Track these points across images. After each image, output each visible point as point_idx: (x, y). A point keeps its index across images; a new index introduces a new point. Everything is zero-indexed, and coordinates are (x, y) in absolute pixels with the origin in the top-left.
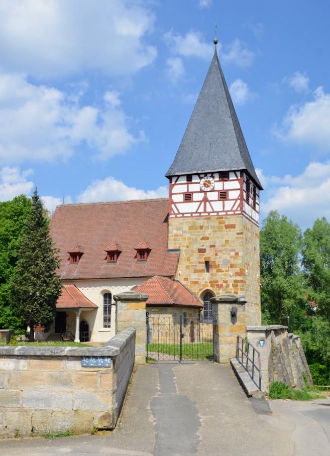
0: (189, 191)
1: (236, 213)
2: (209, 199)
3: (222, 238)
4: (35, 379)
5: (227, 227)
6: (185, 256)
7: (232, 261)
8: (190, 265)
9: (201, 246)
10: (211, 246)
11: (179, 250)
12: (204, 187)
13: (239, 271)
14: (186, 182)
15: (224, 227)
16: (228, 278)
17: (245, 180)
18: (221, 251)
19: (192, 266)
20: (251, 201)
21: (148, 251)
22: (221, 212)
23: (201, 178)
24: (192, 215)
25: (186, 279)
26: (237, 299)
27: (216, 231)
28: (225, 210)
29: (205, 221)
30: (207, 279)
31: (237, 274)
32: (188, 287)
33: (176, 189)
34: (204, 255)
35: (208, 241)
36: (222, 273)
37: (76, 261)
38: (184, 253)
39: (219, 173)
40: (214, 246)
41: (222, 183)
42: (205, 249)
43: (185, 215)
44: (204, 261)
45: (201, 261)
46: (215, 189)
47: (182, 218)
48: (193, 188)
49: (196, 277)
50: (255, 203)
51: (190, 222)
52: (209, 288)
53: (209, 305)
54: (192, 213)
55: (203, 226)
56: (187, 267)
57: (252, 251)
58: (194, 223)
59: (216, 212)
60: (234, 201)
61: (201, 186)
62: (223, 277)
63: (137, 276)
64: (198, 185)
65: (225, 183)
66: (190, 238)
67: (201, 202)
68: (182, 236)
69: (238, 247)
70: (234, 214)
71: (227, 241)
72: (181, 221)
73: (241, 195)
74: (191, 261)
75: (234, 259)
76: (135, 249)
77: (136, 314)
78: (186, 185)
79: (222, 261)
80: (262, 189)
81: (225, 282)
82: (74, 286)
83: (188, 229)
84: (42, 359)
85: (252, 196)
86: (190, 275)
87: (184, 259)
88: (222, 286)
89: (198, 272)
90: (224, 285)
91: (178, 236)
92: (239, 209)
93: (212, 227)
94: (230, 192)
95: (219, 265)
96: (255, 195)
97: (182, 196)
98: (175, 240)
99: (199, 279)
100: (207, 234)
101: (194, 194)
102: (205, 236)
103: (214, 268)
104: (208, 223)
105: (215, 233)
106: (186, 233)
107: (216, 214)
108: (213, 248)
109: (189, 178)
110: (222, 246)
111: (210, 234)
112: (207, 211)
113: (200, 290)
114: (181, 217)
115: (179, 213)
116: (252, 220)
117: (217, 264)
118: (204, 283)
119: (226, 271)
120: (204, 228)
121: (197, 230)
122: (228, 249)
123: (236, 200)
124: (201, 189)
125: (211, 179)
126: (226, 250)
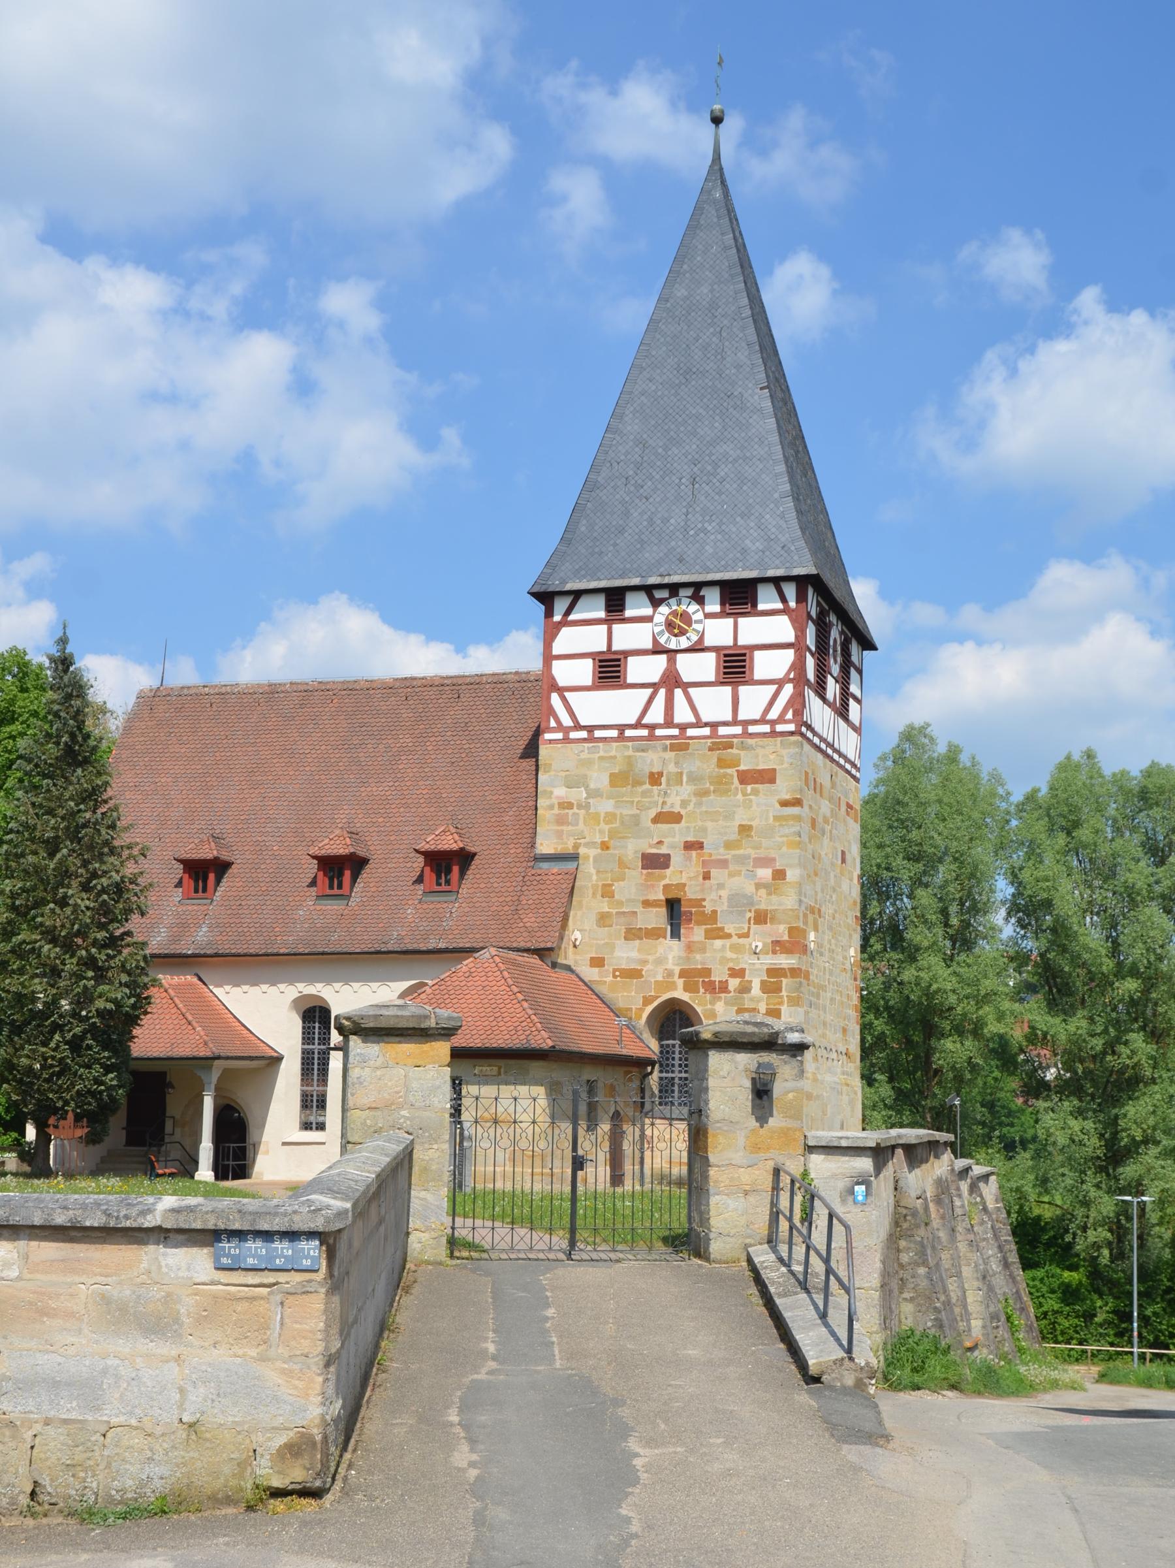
0: (615, 648)
1: (780, 728)
2: (686, 678)
3: (729, 816)
4: (44, 1312)
5: (745, 778)
6: (594, 877)
7: (764, 901)
8: (614, 911)
9: (650, 846)
10: (689, 846)
11: (574, 857)
12: (667, 635)
13: (786, 938)
14: (602, 614)
15: (736, 780)
16: (746, 961)
17: (814, 614)
18: (723, 863)
19: (617, 913)
20: (832, 688)
21: (464, 858)
22: (725, 724)
23: (656, 603)
24: (622, 732)
25: (598, 962)
26: (777, 1034)
27: (706, 793)
28: (741, 717)
29: (670, 755)
30: (670, 961)
31: (778, 946)
32: (602, 990)
33: (566, 641)
34: (665, 877)
36: (727, 942)
37: (205, 890)
38: (593, 871)
39: (723, 585)
40: (699, 846)
41: (730, 621)
42: (667, 857)
43: (598, 734)
44: (662, 898)
45: (652, 897)
46: (708, 642)
48: (628, 636)
49: (634, 954)
50: (845, 694)
51: (615, 757)
53: (677, 1056)
54: (621, 728)
55: (661, 774)
56: (603, 919)
57: (832, 864)
58: (629, 761)
59: (706, 725)
60: (774, 687)
61: (657, 629)
62: (729, 955)
63: (423, 947)
64: (647, 626)
65: (742, 621)
66: (614, 815)
67: (655, 687)
68: (587, 806)
69: (784, 849)
70: (773, 734)
71: (745, 829)
72: (584, 756)
73: (798, 666)
74: (617, 897)
75: (769, 894)
76: (417, 851)
77: (414, 1085)
78: (604, 627)
79: (725, 900)
80: (874, 648)
81: (738, 973)
82: (195, 980)
84: (72, 1240)
85: (835, 669)
86: (612, 947)
87: (590, 892)
89: (642, 939)
90: (734, 983)
91: (570, 806)
92: (789, 716)
93: (693, 779)
94: (758, 655)
95: (715, 912)
96: (846, 666)
97: (588, 665)
98: (561, 821)
99: (646, 962)
100: (674, 802)
101: (631, 660)
103: (699, 923)
104: (677, 763)
105: (704, 799)
106: (601, 796)
107: (706, 731)
108: (694, 853)
109: (615, 600)
110: (728, 845)
111: (684, 803)
113: (647, 1001)
114: (584, 740)
115: (578, 727)
116: (836, 757)
117: (708, 909)
118: (660, 978)
119: (740, 936)
120: (664, 780)
121: (640, 789)
122: (749, 857)
123: (780, 683)
124: (655, 641)
125: (693, 607)
126: (741, 860)
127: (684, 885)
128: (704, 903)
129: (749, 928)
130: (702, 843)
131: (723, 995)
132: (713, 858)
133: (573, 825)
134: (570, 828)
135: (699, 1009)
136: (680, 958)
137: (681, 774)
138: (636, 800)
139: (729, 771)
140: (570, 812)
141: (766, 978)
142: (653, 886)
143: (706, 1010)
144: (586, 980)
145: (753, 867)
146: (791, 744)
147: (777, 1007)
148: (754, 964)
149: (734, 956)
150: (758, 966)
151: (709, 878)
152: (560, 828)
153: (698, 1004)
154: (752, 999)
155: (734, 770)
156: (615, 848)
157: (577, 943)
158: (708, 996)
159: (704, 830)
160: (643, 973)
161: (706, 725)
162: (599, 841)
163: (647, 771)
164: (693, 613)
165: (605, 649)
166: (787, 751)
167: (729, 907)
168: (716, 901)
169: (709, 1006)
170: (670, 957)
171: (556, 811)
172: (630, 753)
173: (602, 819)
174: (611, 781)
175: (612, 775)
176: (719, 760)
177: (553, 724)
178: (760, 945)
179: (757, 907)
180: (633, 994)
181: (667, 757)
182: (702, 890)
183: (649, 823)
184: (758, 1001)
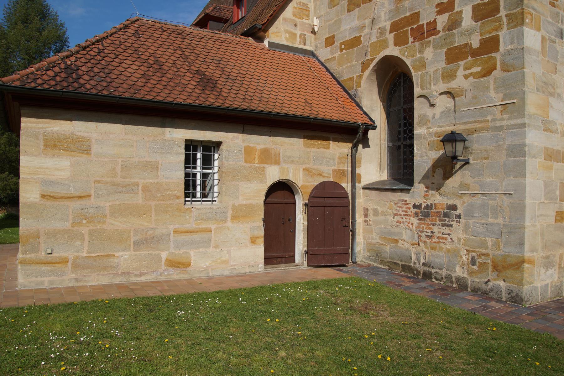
32: (333, 67)
49: (356, 23)
52: (392, 50)
86: (338, 22)
88: (432, 29)
90: (442, 20)
99: (362, 27)
113: (365, 66)
131: (431, 39)
135: (408, 62)
136: (390, 11)
144: (322, 60)
147: (495, 33)
153: (408, 57)
154: (462, 34)
157: (316, 29)
158: (417, 44)
160: (362, 39)
169: (418, 55)
170: (382, 14)
180: (354, 62)
184: (470, 34)
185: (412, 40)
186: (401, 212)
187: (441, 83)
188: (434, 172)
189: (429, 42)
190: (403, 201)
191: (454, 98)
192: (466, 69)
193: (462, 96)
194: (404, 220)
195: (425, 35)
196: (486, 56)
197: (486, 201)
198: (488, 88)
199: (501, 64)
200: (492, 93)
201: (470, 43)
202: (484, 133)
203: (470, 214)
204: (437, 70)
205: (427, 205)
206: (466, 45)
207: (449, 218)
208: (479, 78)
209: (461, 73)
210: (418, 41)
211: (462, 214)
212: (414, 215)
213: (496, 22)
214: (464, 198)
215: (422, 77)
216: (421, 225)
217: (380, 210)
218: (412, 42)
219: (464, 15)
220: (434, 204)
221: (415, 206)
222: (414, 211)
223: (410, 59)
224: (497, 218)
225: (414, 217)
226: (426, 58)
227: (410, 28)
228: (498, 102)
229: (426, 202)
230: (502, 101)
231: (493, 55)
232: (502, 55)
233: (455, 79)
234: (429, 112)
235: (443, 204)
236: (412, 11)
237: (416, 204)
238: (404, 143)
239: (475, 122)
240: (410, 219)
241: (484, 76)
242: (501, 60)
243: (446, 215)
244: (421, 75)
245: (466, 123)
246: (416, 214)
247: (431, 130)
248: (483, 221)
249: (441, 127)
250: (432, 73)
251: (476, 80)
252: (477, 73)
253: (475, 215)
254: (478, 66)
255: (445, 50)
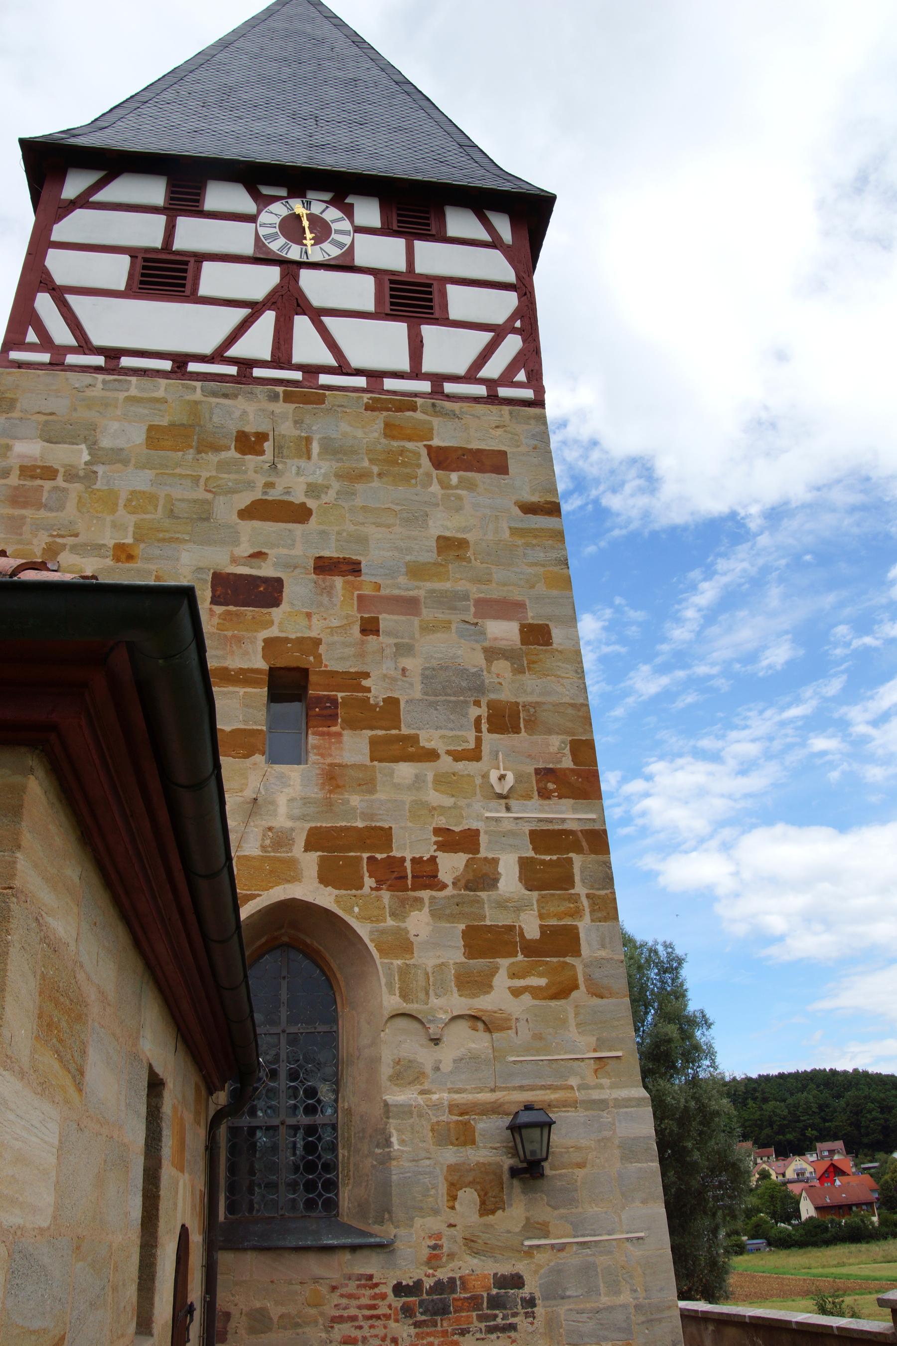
0: (178, 245)
12: (282, 240)
13: (567, 763)
15: (425, 461)
18: (410, 605)
23: (263, 201)
27: (363, 476)
30: (282, 808)
35: (297, 528)
36: (428, 770)
43: (126, 362)
44: (262, 665)
46: (359, 261)
47: (100, 377)
54: (180, 360)
59: (358, 372)
60: (486, 337)
62: (434, 797)
65: (418, 244)
66: (152, 499)
67: (256, 309)
68: (90, 476)
69: (541, 588)
70: (493, 399)
75: (519, 671)
78: (162, 219)
79: (417, 680)
83: (137, 435)
92: (521, 376)
95: (392, 703)
101: (208, 267)
102: (274, 495)
103: (354, 725)
104: (298, 423)
105: (359, 487)
106: (125, 462)
108: (339, 582)
110: (416, 571)
111: (313, 490)
112: (298, 357)
114: (98, 369)
117: (377, 691)
119: (458, 756)
120: (268, 446)
121: (213, 458)
122: (466, 597)
123: (499, 332)
126: (450, 601)
127: (317, 642)
128: (365, 683)
129: (479, 740)
130: (359, 563)
131: (425, 894)
132: (383, 592)
133: (51, 510)
134: (43, 513)
135: (363, 930)
136: (306, 801)
137: (308, 440)
138: (205, 474)
139: (410, 445)
140: (48, 485)
141: (531, 854)
142: (239, 640)
143: (382, 932)
145: (475, 616)
146: (529, 418)
147: (567, 921)
148: (497, 820)
149: (448, 801)
150: (507, 826)
151: (377, 632)
152: (17, 512)
153: (362, 918)
154: (501, 905)
155: (420, 444)
156: (149, 560)
158: (386, 896)
159: (363, 540)
161: (358, 372)
162: (111, 543)
163: (233, 427)
164: (334, 221)
165: (158, 244)
166: (526, 427)
167: (426, 694)
168: (394, 680)
169: (390, 922)
170: (282, 801)
171: (14, 480)
172: (198, 395)
173: (121, 503)
174: (149, 438)
175: (151, 428)
176: (387, 425)
177: (31, 337)
178: (510, 779)
179: (493, 696)
181: (277, 411)
182: (361, 656)
183: (235, 517)
184: (518, 910)
185: (374, 885)
186: (353, 1311)
187: (456, 995)
188: (454, 1198)
189: (419, 900)
190: (360, 1277)
191: (488, 1029)
192: (513, 976)
193: (510, 1031)
194: (366, 1332)
195: (409, 882)
196: (555, 960)
197: (591, 1259)
198: (564, 1022)
199: (586, 980)
200: (572, 1033)
201: (520, 927)
202: (568, 1111)
203: (555, 1293)
204: (443, 964)
205: (439, 1283)
206: (510, 928)
207: (506, 1308)
208: (544, 998)
209: (502, 981)
210: (388, 890)
211: (537, 1295)
212: (396, 1314)
213: (570, 902)
214: (539, 1255)
215: (404, 972)
216: (423, 1339)
217: (275, 1311)
218: (372, 889)
219: (501, 869)
220: (460, 1278)
221: (399, 1290)
222: (398, 1303)
223: (369, 926)
224: (618, 1293)
225: (397, 1321)
226: (412, 932)
227: (365, 855)
228: (588, 1051)
229: (434, 1276)
230: (595, 1050)
231: (568, 960)
232: (586, 966)
233: (488, 993)
234: (425, 1056)
235: (485, 1277)
236: (372, 820)
237: (404, 1283)
238: (291, 1121)
239: (543, 1088)
240: (385, 1327)
241: (555, 997)
242: (584, 972)
243: (496, 1303)
244: (400, 968)
245: (521, 1088)
246: (407, 1311)
247: (435, 1097)
248: (588, 1305)
249: (459, 1091)
250: (430, 970)
251: (537, 1002)
252: (539, 988)
253: (568, 1293)
254: (540, 975)
255: (462, 926)
